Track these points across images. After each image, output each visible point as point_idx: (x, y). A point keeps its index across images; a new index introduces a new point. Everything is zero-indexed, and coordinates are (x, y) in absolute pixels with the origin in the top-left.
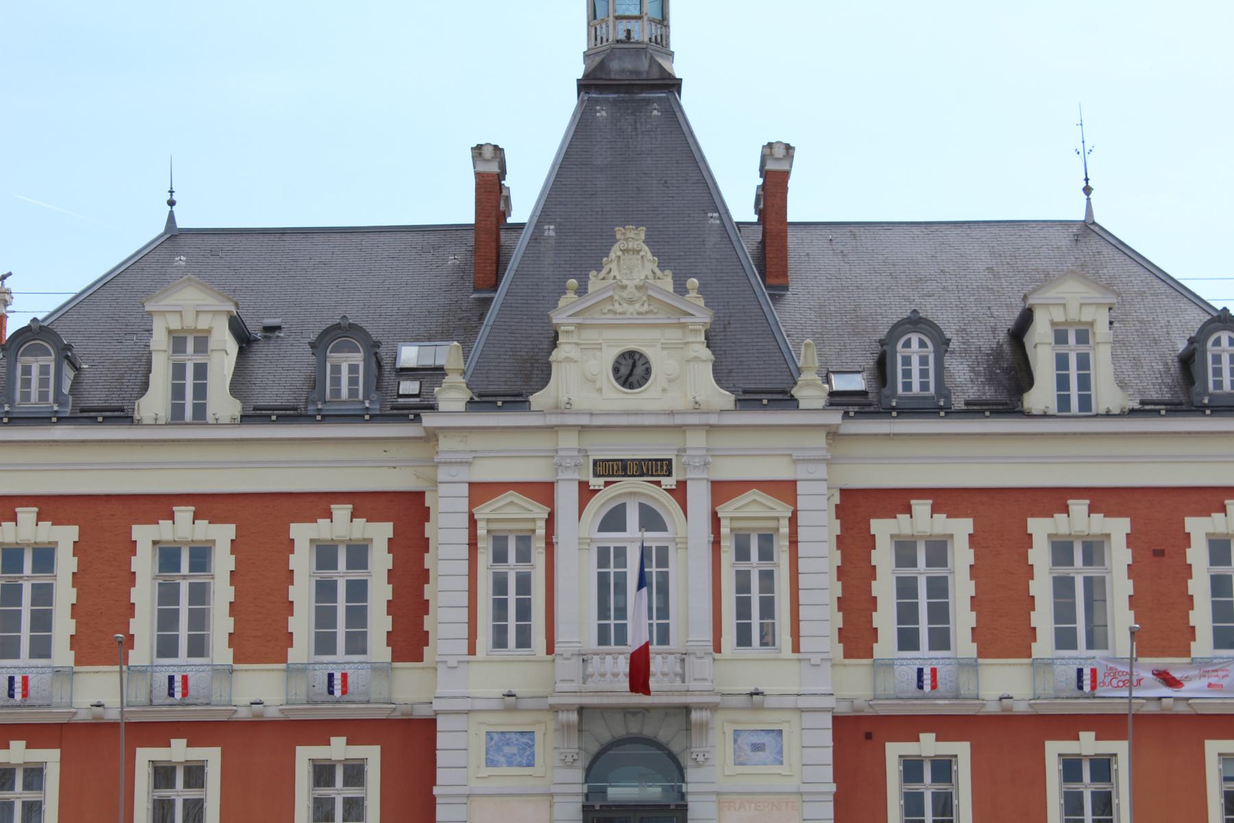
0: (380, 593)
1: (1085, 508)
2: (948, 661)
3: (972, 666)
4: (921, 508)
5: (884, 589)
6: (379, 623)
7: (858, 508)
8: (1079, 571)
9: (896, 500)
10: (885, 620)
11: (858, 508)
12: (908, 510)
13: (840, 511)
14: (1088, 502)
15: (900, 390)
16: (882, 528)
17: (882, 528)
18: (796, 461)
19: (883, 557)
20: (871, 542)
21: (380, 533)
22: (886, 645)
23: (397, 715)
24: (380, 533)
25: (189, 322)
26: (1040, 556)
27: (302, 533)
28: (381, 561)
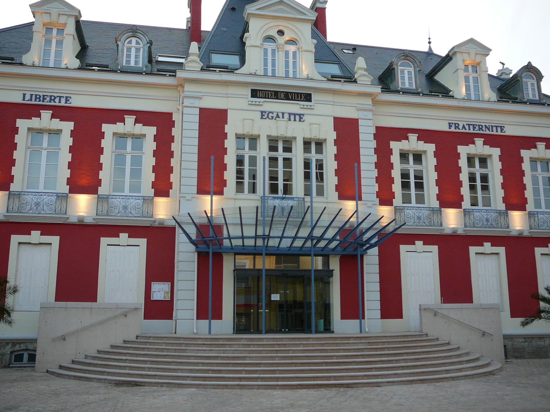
0: (149, 161)
1: (482, 142)
2: (428, 209)
3: (438, 212)
4: (413, 137)
5: (396, 174)
6: (148, 177)
7: (385, 136)
8: (478, 170)
9: (401, 134)
10: (397, 187)
11: (385, 136)
12: (407, 138)
13: (376, 136)
14: (483, 139)
15: (400, 86)
16: (396, 146)
17: (396, 146)
18: (359, 110)
19: (395, 159)
20: (390, 152)
21: (151, 131)
22: (398, 201)
23: (156, 224)
24: (151, 131)
25: (54, 19)
26: (463, 163)
27: (108, 129)
28: (150, 145)
